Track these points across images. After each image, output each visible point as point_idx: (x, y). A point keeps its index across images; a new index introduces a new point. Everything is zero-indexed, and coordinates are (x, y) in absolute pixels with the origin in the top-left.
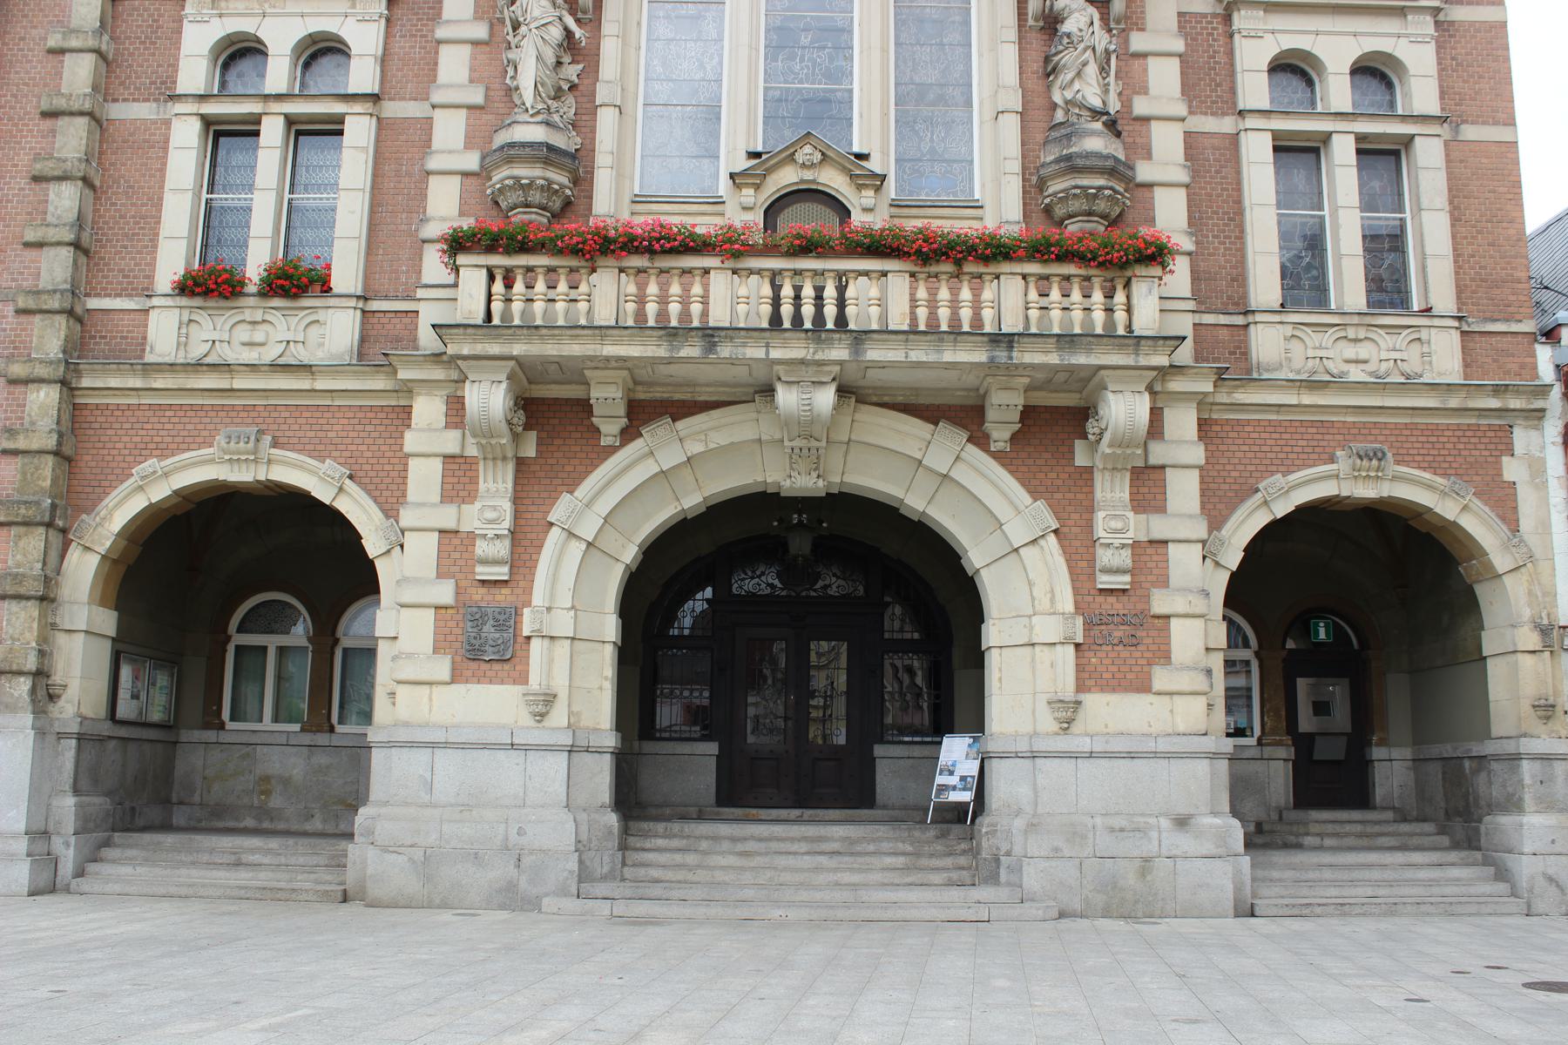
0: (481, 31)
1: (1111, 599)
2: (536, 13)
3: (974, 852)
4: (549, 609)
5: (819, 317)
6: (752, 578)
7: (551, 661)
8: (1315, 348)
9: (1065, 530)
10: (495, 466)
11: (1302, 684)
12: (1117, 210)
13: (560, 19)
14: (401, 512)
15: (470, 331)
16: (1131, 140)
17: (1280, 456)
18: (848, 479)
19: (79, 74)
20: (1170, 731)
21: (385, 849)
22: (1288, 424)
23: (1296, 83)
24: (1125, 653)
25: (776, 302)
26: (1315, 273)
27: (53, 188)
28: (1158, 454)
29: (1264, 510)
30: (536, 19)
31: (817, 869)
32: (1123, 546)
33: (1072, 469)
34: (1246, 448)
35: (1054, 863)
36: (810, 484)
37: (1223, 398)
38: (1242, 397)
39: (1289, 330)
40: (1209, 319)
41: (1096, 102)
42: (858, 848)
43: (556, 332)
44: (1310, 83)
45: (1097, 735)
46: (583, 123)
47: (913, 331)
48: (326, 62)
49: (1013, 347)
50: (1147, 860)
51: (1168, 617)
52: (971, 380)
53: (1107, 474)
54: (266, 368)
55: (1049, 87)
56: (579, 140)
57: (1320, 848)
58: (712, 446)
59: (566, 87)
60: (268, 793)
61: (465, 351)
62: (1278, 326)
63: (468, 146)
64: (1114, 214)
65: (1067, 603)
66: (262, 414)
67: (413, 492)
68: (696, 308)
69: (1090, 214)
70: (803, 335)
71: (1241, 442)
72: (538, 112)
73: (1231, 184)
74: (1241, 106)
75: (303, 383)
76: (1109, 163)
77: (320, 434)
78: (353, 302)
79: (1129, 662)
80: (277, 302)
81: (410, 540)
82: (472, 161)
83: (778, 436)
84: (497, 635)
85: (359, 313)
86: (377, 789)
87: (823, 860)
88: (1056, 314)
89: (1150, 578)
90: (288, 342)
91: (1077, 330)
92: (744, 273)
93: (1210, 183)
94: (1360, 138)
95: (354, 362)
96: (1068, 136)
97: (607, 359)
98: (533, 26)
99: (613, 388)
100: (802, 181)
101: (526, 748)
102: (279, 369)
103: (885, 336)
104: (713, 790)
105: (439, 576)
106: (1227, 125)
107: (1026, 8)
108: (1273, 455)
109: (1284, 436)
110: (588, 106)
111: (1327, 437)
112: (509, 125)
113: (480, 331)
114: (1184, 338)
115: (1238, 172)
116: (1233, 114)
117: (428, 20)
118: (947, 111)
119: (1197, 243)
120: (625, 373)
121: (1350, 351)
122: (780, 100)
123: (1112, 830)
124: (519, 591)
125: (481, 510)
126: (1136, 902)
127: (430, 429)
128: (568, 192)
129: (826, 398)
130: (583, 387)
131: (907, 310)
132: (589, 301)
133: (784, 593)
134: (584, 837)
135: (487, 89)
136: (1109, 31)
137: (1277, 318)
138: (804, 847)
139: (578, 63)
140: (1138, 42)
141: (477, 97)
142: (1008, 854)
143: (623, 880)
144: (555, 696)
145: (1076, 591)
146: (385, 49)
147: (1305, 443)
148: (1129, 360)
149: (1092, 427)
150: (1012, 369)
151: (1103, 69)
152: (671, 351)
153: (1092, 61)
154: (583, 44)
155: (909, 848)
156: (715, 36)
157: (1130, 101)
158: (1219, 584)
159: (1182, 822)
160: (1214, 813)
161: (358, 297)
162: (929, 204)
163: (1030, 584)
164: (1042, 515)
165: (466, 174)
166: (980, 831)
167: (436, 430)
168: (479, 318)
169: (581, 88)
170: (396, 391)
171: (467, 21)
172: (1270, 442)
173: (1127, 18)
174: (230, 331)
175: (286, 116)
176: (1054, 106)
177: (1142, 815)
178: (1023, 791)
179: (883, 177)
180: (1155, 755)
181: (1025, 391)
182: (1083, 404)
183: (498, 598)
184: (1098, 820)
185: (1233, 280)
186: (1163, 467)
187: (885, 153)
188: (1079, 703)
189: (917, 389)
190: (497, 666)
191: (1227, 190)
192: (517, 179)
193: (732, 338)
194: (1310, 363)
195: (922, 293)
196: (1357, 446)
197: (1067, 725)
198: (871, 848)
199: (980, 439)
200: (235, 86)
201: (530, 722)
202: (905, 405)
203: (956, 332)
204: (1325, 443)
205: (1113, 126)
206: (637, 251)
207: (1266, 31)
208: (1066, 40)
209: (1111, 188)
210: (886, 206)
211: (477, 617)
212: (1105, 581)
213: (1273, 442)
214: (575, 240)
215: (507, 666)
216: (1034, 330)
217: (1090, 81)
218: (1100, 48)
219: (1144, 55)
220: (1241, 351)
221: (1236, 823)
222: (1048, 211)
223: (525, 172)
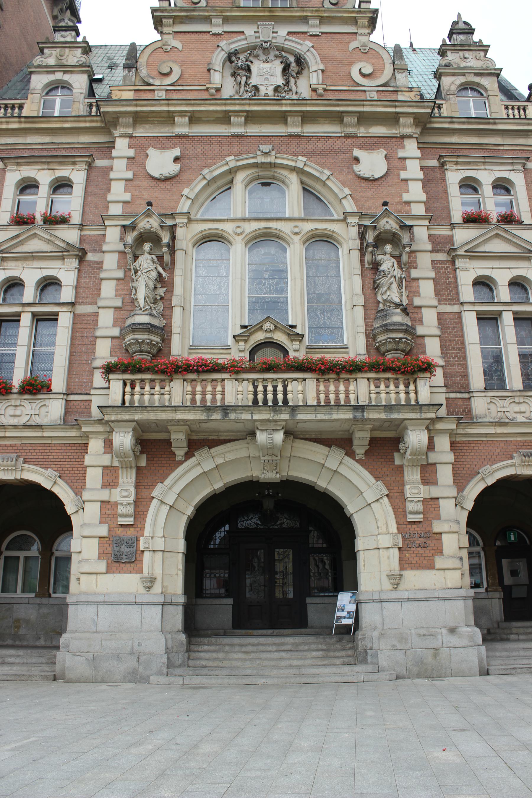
0: (120, 274)
1: (414, 526)
2: (145, 266)
3: (355, 648)
4: (152, 538)
5: (275, 400)
6: (247, 520)
7: (153, 562)
8: (501, 407)
9: (392, 494)
10: (127, 471)
11: (505, 562)
12: (409, 348)
13: (156, 268)
14: (83, 493)
15: (115, 409)
16: (413, 316)
17: (488, 457)
18: (291, 473)
20: (444, 587)
21: (75, 654)
22: (491, 442)
23: (485, 290)
24: (422, 551)
25: (255, 393)
26: (499, 373)
28: (433, 458)
29: (482, 482)
30: (145, 268)
31: (281, 659)
32: (419, 501)
33: (393, 466)
34: (473, 454)
35: (392, 652)
36: (273, 477)
37: (461, 431)
38: (469, 430)
39: (489, 399)
40: (452, 395)
41: (397, 300)
42: (300, 648)
43: (155, 409)
44: (491, 290)
45: (410, 590)
46: (166, 314)
47: (318, 405)
48: (51, 289)
49: (364, 411)
50: (437, 649)
51: (441, 533)
52: (346, 427)
53: (410, 468)
54: (21, 427)
55: (376, 294)
56: (165, 322)
57: (518, 640)
58: (227, 460)
59: (158, 298)
60: (18, 627)
61: (113, 418)
62: (484, 398)
63: (114, 325)
64: (408, 350)
65: (394, 528)
66: (19, 448)
67: (89, 483)
68: (219, 397)
69: (397, 350)
70: (268, 408)
71: (470, 451)
72: (146, 310)
73: (459, 335)
74: (461, 300)
75: (39, 434)
76: (405, 327)
77: (46, 457)
78: (61, 396)
79: (424, 555)
80: (27, 397)
81: (87, 506)
82: (116, 332)
83: (257, 455)
84: (128, 550)
85: (64, 401)
86: (71, 624)
87: (283, 654)
88: (383, 396)
89: (432, 515)
90: (31, 415)
91: (393, 403)
92: (241, 380)
93: (450, 335)
94: (515, 313)
95: (62, 424)
96: (385, 316)
97: (178, 421)
98: (143, 272)
99: (181, 434)
100: (266, 338)
101: (142, 604)
102: (27, 427)
103: (306, 408)
104: (231, 621)
105: (101, 522)
106: (456, 309)
107: (364, 260)
108: (485, 457)
109: (490, 448)
110: (169, 306)
111: (509, 447)
112: (133, 315)
113: (120, 409)
114: (442, 405)
115: (462, 330)
116: (458, 304)
117: (97, 269)
118: (330, 306)
119: (445, 361)
120: (187, 427)
121: (517, 408)
122: (255, 302)
123: (420, 635)
124: (138, 529)
125: (120, 492)
126: (433, 670)
127: (96, 454)
128: (160, 345)
129: (279, 437)
130: (167, 434)
131: (316, 396)
132: (170, 394)
133: (262, 527)
134: (170, 646)
135: (123, 299)
136: (401, 269)
137: (483, 394)
138: (274, 648)
139: (164, 287)
140: (414, 273)
141: (118, 303)
142: (371, 648)
143: (189, 666)
144: (155, 579)
145: (398, 523)
146: (77, 283)
147: (499, 451)
148: (417, 416)
149: (402, 447)
150: (364, 421)
151: (400, 285)
152: (207, 417)
153: (394, 282)
154: (166, 279)
155: (324, 647)
156: (225, 274)
157: (412, 299)
158: (464, 517)
159: (452, 631)
160: (467, 626)
161: (64, 394)
162: (324, 347)
163: (377, 520)
164: (380, 488)
165: (113, 338)
166: (357, 638)
167: (99, 455)
168: (119, 404)
169: (165, 298)
170: (81, 437)
171: (114, 270)
172: (483, 451)
173: (409, 263)
174: (5, 410)
175: (32, 313)
176: (379, 302)
177: (434, 628)
178: (377, 619)
179: (303, 336)
180: (438, 599)
181: (371, 431)
182: (397, 436)
183: (129, 532)
184: (413, 631)
185: (463, 377)
186: (435, 464)
187: (303, 325)
188: (401, 575)
189: (321, 431)
190: (128, 565)
191: (458, 337)
192: (137, 340)
193: (235, 410)
194: (499, 414)
195: (322, 388)
196: (523, 451)
197: (396, 586)
198: (306, 648)
199: (351, 454)
200: (8, 301)
201: (142, 591)
202: (316, 439)
203: (338, 405)
204: (508, 450)
205: (405, 311)
206: (192, 371)
207: (470, 268)
208: (382, 274)
209: (406, 338)
210: (305, 348)
211: (119, 542)
212: (411, 518)
213: (484, 451)
214: (163, 367)
215: (132, 565)
216: (373, 403)
217: (393, 291)
218: (398, 277)
219: (417, 279)
220: (468, 409)
221: (478, 630)
222: (378, 349)
223: (140, 336)
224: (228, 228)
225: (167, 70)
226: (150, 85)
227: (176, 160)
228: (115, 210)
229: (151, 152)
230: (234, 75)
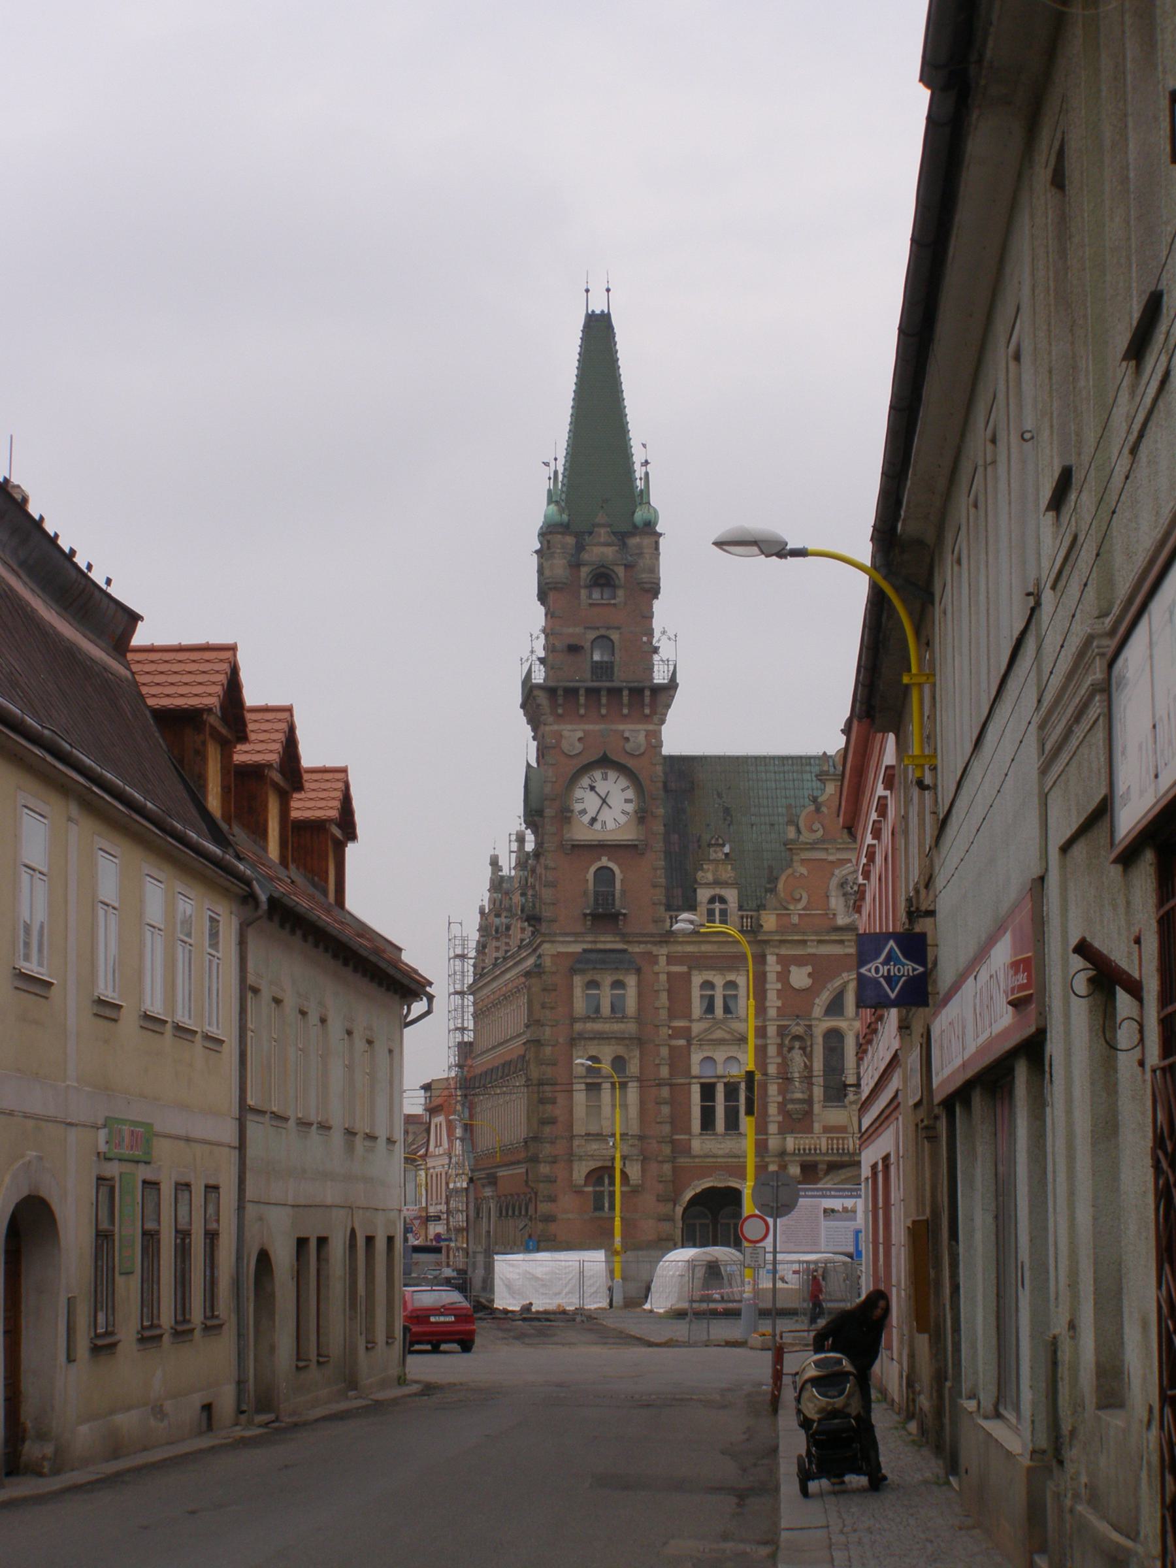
0: (779, 1060)
19: (665, 1072)
27: (662, 1106)
75: (736, 1160)
82: (780, 1099)
224: (842, 1024)
225: (798, 897)
226: (787, 909)
227: (810, 975)
228: (772, 1013)
229: (793, 969)
230: (845, 895)
